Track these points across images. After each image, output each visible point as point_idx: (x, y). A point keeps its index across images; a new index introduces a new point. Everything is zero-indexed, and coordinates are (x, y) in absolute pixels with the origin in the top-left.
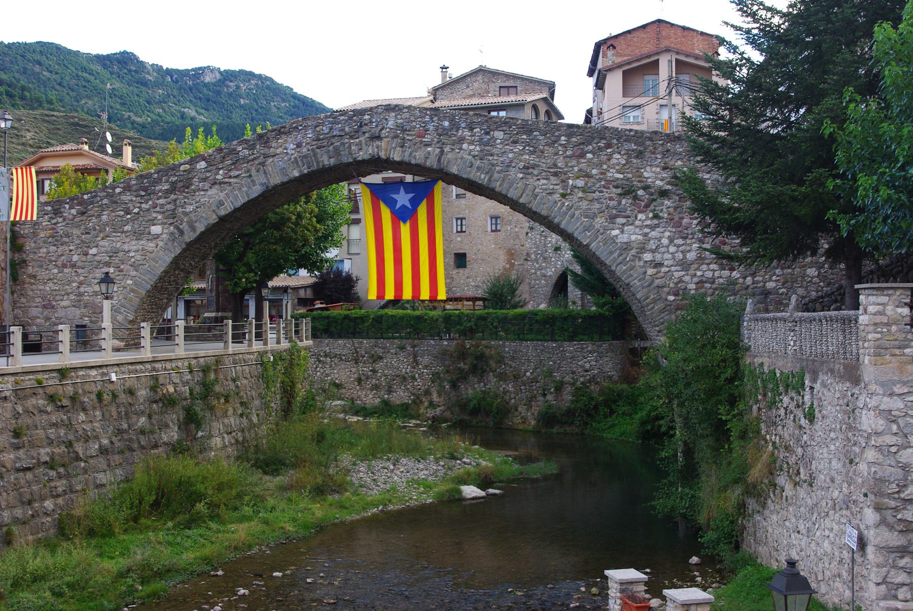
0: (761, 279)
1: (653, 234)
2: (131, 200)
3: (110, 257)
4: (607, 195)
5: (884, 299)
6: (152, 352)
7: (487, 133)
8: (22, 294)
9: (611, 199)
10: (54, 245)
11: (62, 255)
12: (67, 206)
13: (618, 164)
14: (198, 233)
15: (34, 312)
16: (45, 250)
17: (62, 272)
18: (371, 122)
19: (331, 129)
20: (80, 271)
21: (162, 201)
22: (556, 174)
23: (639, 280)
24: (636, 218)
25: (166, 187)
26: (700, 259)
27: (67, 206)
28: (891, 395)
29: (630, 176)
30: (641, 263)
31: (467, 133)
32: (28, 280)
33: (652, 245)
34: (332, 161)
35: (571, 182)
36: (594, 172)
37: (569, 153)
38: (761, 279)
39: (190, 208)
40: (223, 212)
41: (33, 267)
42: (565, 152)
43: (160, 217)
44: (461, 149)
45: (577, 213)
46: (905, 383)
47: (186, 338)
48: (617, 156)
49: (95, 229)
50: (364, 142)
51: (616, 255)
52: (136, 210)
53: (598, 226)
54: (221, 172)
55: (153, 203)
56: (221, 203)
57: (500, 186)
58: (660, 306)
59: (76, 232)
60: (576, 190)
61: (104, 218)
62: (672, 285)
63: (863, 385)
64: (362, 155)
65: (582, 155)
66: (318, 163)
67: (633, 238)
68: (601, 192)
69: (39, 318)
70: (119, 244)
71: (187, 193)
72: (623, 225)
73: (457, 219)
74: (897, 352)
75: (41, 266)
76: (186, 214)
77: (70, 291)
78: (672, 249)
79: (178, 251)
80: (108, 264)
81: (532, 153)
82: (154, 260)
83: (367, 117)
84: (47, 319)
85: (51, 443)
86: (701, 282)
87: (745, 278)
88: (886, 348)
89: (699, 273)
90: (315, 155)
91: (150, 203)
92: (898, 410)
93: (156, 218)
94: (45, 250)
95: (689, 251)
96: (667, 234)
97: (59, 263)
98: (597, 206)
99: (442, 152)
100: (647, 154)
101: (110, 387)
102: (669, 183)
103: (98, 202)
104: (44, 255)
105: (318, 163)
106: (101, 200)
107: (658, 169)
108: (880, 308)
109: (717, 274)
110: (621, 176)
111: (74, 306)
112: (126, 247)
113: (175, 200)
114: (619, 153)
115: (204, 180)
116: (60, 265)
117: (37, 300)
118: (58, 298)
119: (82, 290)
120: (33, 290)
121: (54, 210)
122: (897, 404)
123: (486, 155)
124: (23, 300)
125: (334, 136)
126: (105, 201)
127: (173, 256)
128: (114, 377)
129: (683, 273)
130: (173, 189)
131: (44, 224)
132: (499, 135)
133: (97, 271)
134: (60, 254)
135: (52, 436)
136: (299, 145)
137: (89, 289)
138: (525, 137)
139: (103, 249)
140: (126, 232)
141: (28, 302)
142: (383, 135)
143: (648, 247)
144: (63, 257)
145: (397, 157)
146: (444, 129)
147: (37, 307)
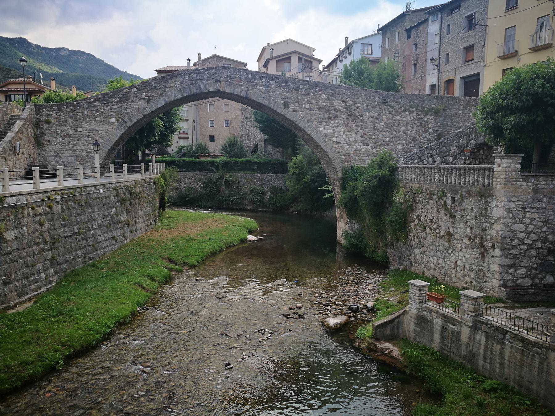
0: (379, 150)
1: (337, 130)
2: (99, 106)
3: (89, 133)
4: (318, 112)
5: (511, 161)
6: (115, 179)
7: (268, 82)
8: (43, 150)
9: (320, 114)
10: (59, 126)
11: (64, 131)
12: (65, 107)
13: (324, 99)
14: (133, 122)
15: (50, 159)
16: (54, 128)
17: (64, 139)
18: (216, 74)
19: (197, 76)
20: (74, 139)
21: (115, 107)
22: (297, 102)
23: (331, 150)
24: (330, 122)
25: (117, 100)
26: (355, 141)
27: (65, 107)
28: (510, 202)
29: (329, 104)
30: (332, 142)
31: (259, 81)
32: (46, 143)
33: (336, 134)
34: (198, 91)
35: (304, 106)
36: (314, 102)
37: (303, 93)
38: (379, 150)
39: (129, 111)
40: (145, 113)
41: (48, 137)
42: (301, 92)
43: (114, 114)
44: (256, 88)
45: (306, 120)
46: (516, 197)
47: (128, 172)
48: (323, 95)
49: (80, 119)
50: (212, 82)
51: (321, 139)
52: (102, 110)
53: (314, 126)
54: (144, 94)
55: (111, 107)
56: (144, 109)
57: (273, 106)
58: (339, 160)
59: (70, 120)
60: (305, 109)
61: (86, 113)
62: (344, 152)
63: (494, 197)
64: (211, 89)
65: (309, 94)
66: (191, 91)
67: (329, 131)
68: (316, 111)
69: (53, 161)
70: (93, 127)
71: (127, 103)
72: (325, 126)
73: (210, 121)
74: (514, 183)
75: (53, 136)
76: (127, 113)
77: (68, 149)
78: (344, 136)
79: (124, 131)
80: (88, 136)
81: (287, 92)
82: (111, 135)
83: (214, 71)
84: (57, 162)
85: (78, 223)
86: (356, 150)
87: (372, 149)
88: (510, 182)
89: (355, 147)
90: (189, 88)
91: (109, 107)
92: (513, 208)
93: (112, 115)
94: (54, 128)
95: (351, 137)
96: (343, 130)
97: (62, 135)
98: (314, 117)
99: (248, 90)
100: (337, 95)
101: (100, 195)
102: (344, 108)
103: (82, 106)
104: (54, 131)
105: (191, 91)
106: (83, 105)
107: (340, 102)
108: (509, 164)
109: (362, 147)
110: (325, 104)
111: (71, 156)
112: (97, 128)
113: (121, 106)
114: (324, 94)
115: (136, 97)
116: (63, 136)
117: (51, 153)
118: (62, 152)
119: (75, 148)
120: (48, 148)
121: (58, 108)
122: (513, 205)
123: (267, 92)
124: (43, 153)
125: (198, 79)
126: (86, 105)
127: (121, 133)
128: (101, 191)
129: (348, 147)
130: (120, 101)
131: (53, 115)
132: (273, 83)
133: (83, 139)
134: (62, 130)
135: (79, 220)
136: (182, 83)
137: (79, 148)
138: (285, 84)
139: (85, 129)
140: (97, 121)
141: (46, 154)
142: (221, 80)
143: (335, 135)
144: (64, 132)
145: (228, 90)
146: (249, 79)
147: (51, 156)
